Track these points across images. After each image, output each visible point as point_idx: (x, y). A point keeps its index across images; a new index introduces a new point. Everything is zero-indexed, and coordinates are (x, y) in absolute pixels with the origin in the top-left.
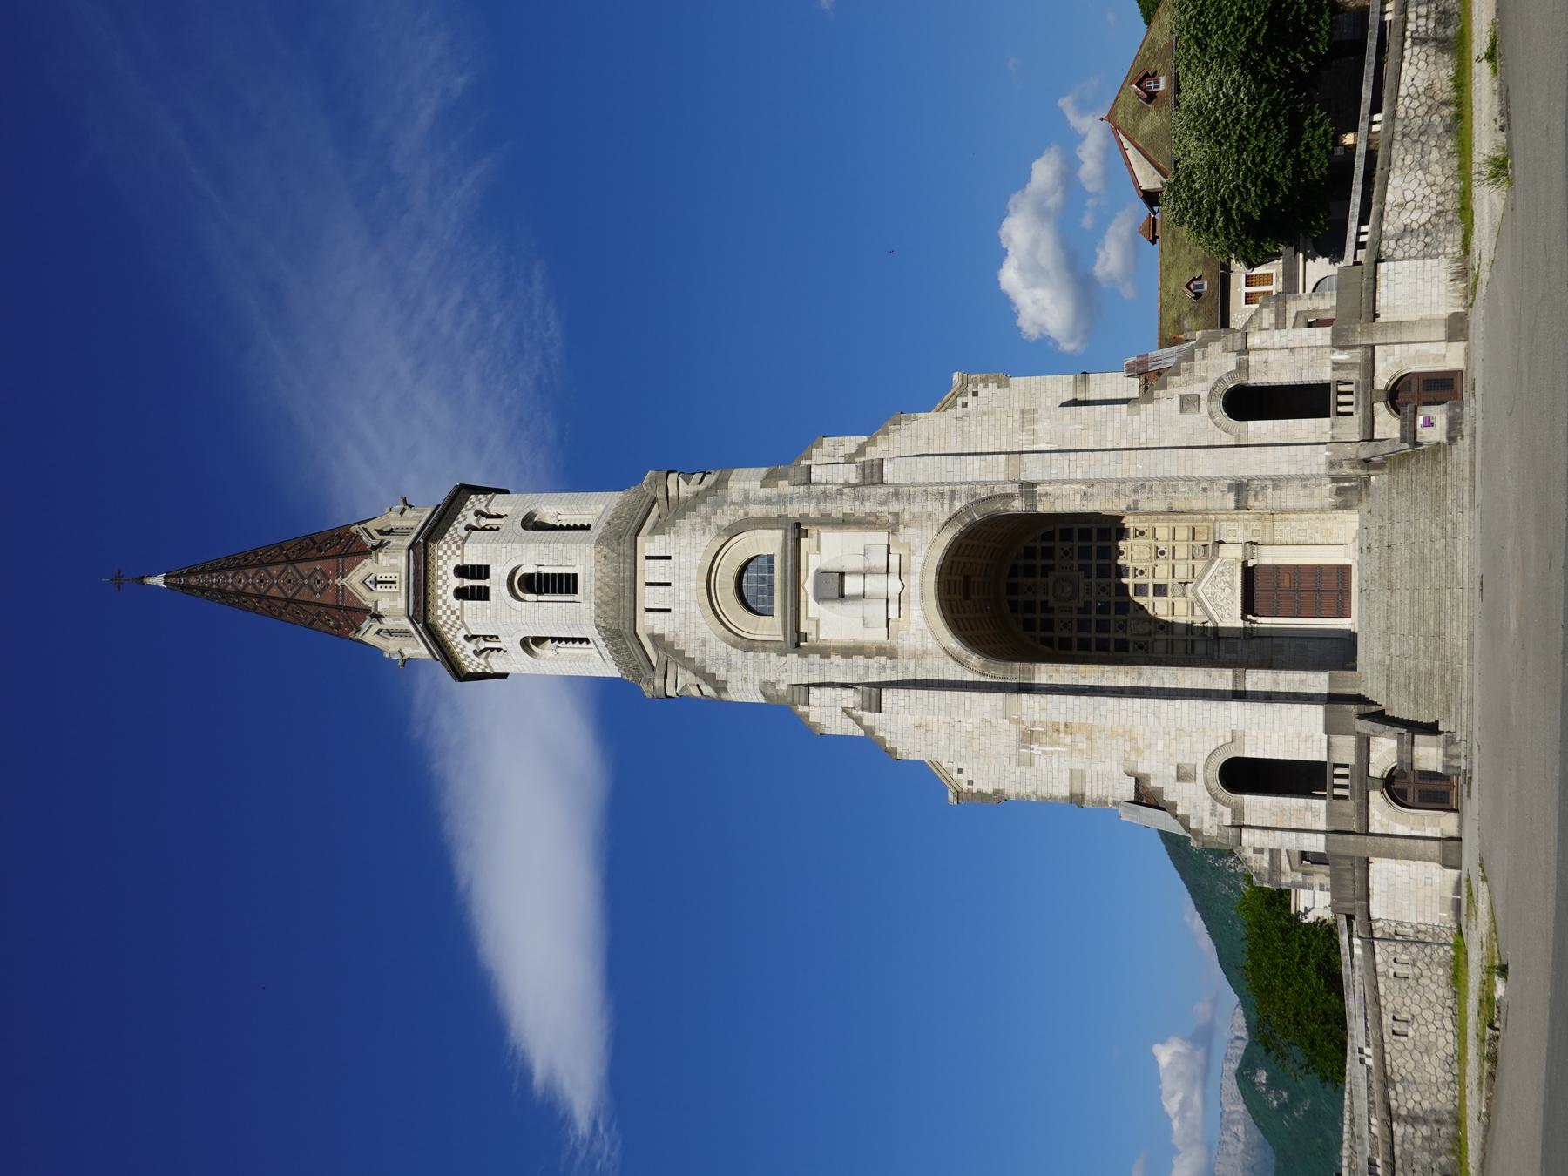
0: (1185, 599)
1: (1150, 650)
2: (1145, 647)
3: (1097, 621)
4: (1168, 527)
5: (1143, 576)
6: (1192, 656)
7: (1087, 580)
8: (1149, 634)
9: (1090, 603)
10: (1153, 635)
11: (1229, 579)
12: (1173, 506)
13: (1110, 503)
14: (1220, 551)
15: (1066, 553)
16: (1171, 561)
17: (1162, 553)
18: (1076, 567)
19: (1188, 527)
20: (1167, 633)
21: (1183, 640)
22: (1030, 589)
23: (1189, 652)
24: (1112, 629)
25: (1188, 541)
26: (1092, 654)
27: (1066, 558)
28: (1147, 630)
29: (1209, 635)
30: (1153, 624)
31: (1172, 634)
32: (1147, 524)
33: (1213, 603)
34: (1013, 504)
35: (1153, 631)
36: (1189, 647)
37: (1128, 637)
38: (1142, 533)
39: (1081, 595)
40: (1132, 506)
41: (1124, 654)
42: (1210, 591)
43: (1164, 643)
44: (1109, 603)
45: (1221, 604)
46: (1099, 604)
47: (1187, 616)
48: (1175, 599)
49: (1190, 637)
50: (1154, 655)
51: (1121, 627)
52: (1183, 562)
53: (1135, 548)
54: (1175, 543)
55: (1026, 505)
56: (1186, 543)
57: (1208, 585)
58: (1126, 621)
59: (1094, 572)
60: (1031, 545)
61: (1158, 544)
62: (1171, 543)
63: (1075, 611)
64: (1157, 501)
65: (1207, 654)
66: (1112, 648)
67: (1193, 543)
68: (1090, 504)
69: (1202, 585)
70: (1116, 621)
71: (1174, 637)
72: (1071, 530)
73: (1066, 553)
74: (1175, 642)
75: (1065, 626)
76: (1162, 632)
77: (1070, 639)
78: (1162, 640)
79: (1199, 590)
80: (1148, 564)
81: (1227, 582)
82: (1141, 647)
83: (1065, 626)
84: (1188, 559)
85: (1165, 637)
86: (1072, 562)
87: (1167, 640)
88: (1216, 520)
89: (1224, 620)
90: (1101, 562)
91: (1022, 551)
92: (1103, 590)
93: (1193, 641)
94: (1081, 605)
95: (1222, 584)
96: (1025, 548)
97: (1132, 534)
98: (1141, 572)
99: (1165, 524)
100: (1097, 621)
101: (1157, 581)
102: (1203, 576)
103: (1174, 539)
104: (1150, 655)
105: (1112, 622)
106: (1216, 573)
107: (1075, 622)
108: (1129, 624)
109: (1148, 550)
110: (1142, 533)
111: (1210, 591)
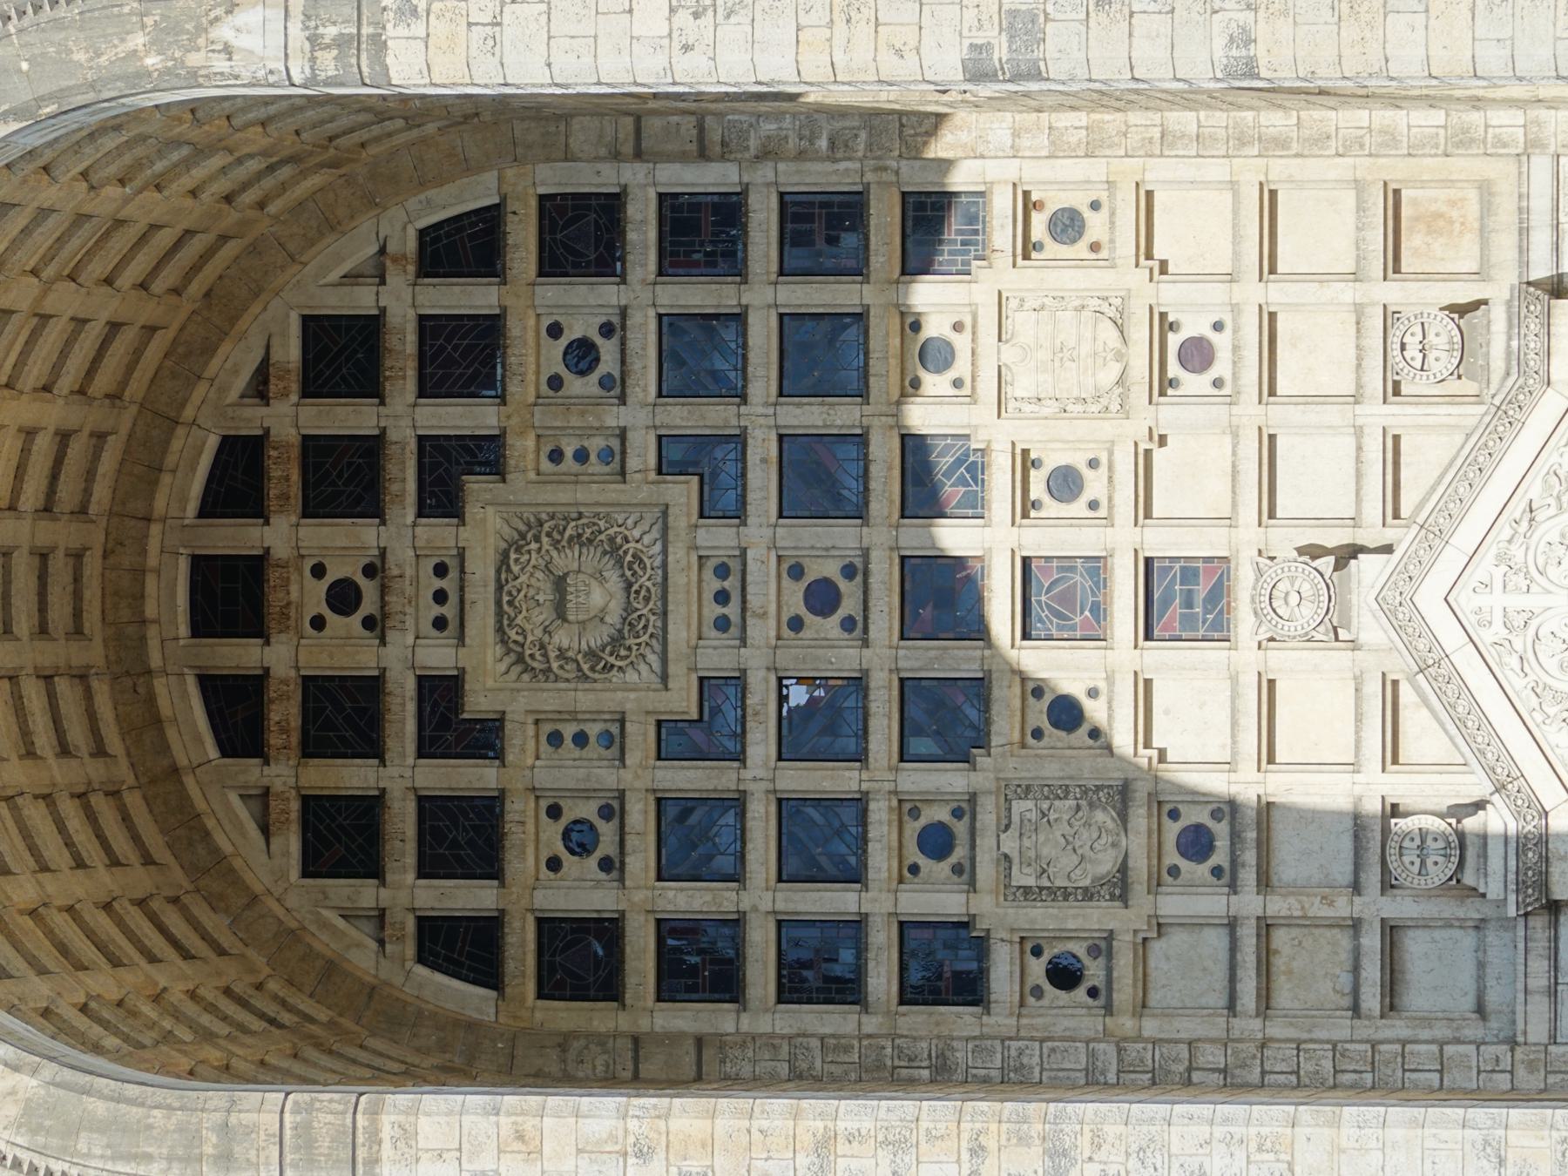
0: (1341, 658)
1: (1124, 994)
2: (1094, 972)
3: (788, 808)
4: (1233, 186)
5: (1078, 508)
6: (1398, 1028)
7: (719, 537)
8: (1119, 886)
9: (739, 681)
10: (1139, 889)
12: (1260, 51)
13: (863, 31)
15: (582, 355)
16: (1250, 412)
17: (1198, 354)
18: (643, 453)
19: (1359, 186)
20: (1228, 878)
21: (1335, 924)
22: (343, 597)
23: (1371, 1000)
24: (880, 861)
25: (1356, 276)
26: (746, 1023)
27: (577, 386)
29: (1494, 889)
30: (1140, 818)
31: (1265, 882)
32: (1096, 169)
33: (1516, 683)
34: (224, 32)
35: (1140, 866)
36: (1372, 972)
37: (988, 908)
38: (1068, 225)
39: (679, 634)
40: (1001, 51)
41: (959, 1019)
42: (1496, 601)
43: (1216, 941)
44: (859, 683)
46: (798, 696)
47: (1355, 766)
48: (1279, 661)
49: (1375, 906)
50: (1150, 1027)
51: (937, 842)
52: (1333, 414)
53: (1020, 322)
54: (1277, 294)
55: (314, 40)
56: (1347, 293)
57: (1486, 567)
58: (967, 808)
59: (762, 482)
60: (362, 301)
61: (1170, 295)
62: (1251, 293)
63: (641, 738)
64: (1161, 24)
65: (1481, 1010)
66: (882, 979)
67: (1392, 293)
68: (733, 32)
70: (908, 807)
71: (1277, 906)
72: (611, 207)
73: (582, 355)
74: (1280, 938)
75: (579, 839)
77: (609, 930)
78: (1196, 925)
79: (1429, 598)
80: (1107, 429)
82: (1064, 976)
83: (579, 839)
84: (1356, 399)
85: (1213, 904)
86: (614, 417)
87: (1232, 925)
88: (1533, 145)
90: (809, 416)
91: (290, 352)
92: (823, 598)
93: (1392, 932)
94: (682, 700)
96: (316, 328)
97: (1002, 234)
98: (1066, 483)
99: (1217, 170)
100: (788, 808)
101: (1162, 542)
102: (1453, 508)
103: (1270, 265)
104: (1125, 1023)
105: (879, 812)
106: (1534, 489)
107: (640, 816)
108: (988, 816)
109: (1109, 334)
110: (1068, 225)
111: (1496, 601)
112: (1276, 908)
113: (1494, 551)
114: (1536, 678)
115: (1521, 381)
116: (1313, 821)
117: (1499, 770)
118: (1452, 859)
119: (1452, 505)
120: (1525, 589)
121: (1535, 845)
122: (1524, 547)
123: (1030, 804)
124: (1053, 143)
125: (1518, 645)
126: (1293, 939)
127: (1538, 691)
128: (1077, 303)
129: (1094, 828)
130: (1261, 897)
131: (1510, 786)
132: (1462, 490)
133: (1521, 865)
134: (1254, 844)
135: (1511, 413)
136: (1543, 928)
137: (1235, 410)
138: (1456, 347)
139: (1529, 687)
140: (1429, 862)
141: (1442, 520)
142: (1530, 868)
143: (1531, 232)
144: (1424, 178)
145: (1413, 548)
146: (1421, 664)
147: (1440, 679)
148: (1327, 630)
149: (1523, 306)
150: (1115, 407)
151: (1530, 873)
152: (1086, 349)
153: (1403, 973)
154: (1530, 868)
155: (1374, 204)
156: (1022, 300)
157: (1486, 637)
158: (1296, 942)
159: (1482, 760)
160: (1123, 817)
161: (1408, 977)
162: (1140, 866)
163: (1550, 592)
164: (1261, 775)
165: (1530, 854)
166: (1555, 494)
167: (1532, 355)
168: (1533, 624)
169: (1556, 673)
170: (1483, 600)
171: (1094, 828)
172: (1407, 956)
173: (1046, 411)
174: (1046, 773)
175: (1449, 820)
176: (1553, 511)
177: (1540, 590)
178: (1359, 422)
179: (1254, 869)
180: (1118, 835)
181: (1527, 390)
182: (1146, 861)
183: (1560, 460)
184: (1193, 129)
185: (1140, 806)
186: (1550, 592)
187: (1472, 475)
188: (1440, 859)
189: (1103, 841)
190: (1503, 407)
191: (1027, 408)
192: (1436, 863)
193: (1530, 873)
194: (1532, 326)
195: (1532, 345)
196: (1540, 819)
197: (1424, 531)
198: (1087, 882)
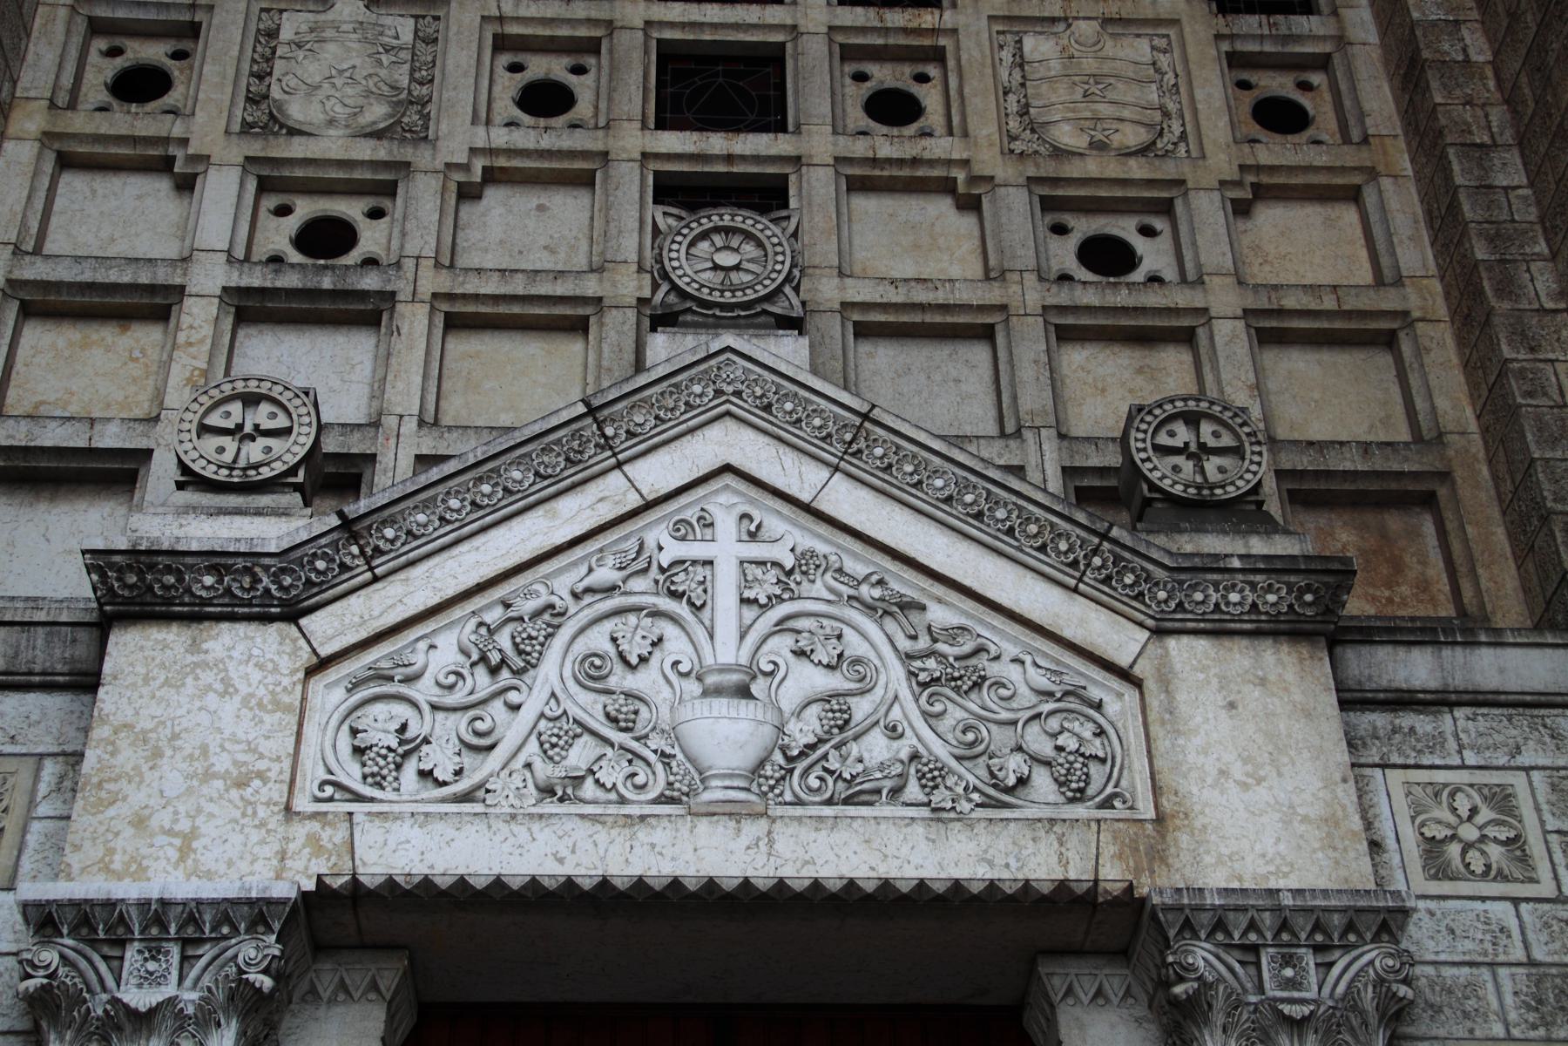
11: (876, 748)
14: (1239, 656)
28: (297, 111)
33: (562, 580)
42: (726, 548)
45: (552, 669)
69: (802, 477)
74: (147, 336)
76: (279, 235)
78: (187, 228)
80: (985, 129)
81: (841, 726)
89: (329, 695)
95: (807, 679)
106: (939, 615)
109: (1133, 136)
111: (726, 548)
112: (195, 310)
113: (822, 548)
114: (572, 611)
115: (1160, 574)
116: (343, 380)
117: (389, 533)
118: (226, 472)
119: (909, 468)
120: (748, 594)
121: (228, 591)
122: (832, 597)
123: (407, 36)
124: (1434, 24)
125: (638, 584)
126: (143, 351)
127: (546, 617)
128: (1172, 107)
129: (361, 101)
130: (218, 292)
131: (355, 549)
132: (939, 483)
133: (189, 560)
134: (309, 285)
135: (1097, 561)
136: (73, 660)
137: (1031, 279)
138: (1206, 492)
139: (555, 599)
140: (230, 444)
141: (879, 451)
142: (180, 580)
143: (1429, 650)
144: (1469, 529)
145: (823, 403)
146: (606, 412)
147: (575, 444)
148: (671, 305)
149: (1313, 580)
150: (1018, 146)
151: (171, 579)
152: (1105, 109)
153: (52, 500)
154: (180, 580)
155: (1406, 459)
156: (1165, 52)
157: (657, 534)
158: (137, 354)
159: (410, 503)
160: (378, 135)
161: (42, 506)
162: (298, 148)
163: (742, 637)
164: (428, 297)
165: (209, 580)
166: (942, 647)
167: (1214, 597)
168: (681, 609)
169: (580, 647)
170: (727, 525)
171: (361, 101)
172: (81, 505)
173: (1004, 74)
174: (453, 50)
175: (301, 473)
176: (905, 644)
177: (748, 622)
178: (1028, 435)
179: (268, 284)
180: (347, 126)
181: (1144, 587)
182: (301, 155)
183: (1006, 658)
184: (1501, 180)
185: (390, 152)
186: (742, 637)
187: (969, 498)
188: (228, 457)
189: (338, 108)
190: (1106, 545)
191: (1007, 55)
192: (221, 450)
193: (171, 579)
194: (1272, 598)
195: (1234, 597)
196: (282, 603)
197: (858, 421)
198: (276, 93)
